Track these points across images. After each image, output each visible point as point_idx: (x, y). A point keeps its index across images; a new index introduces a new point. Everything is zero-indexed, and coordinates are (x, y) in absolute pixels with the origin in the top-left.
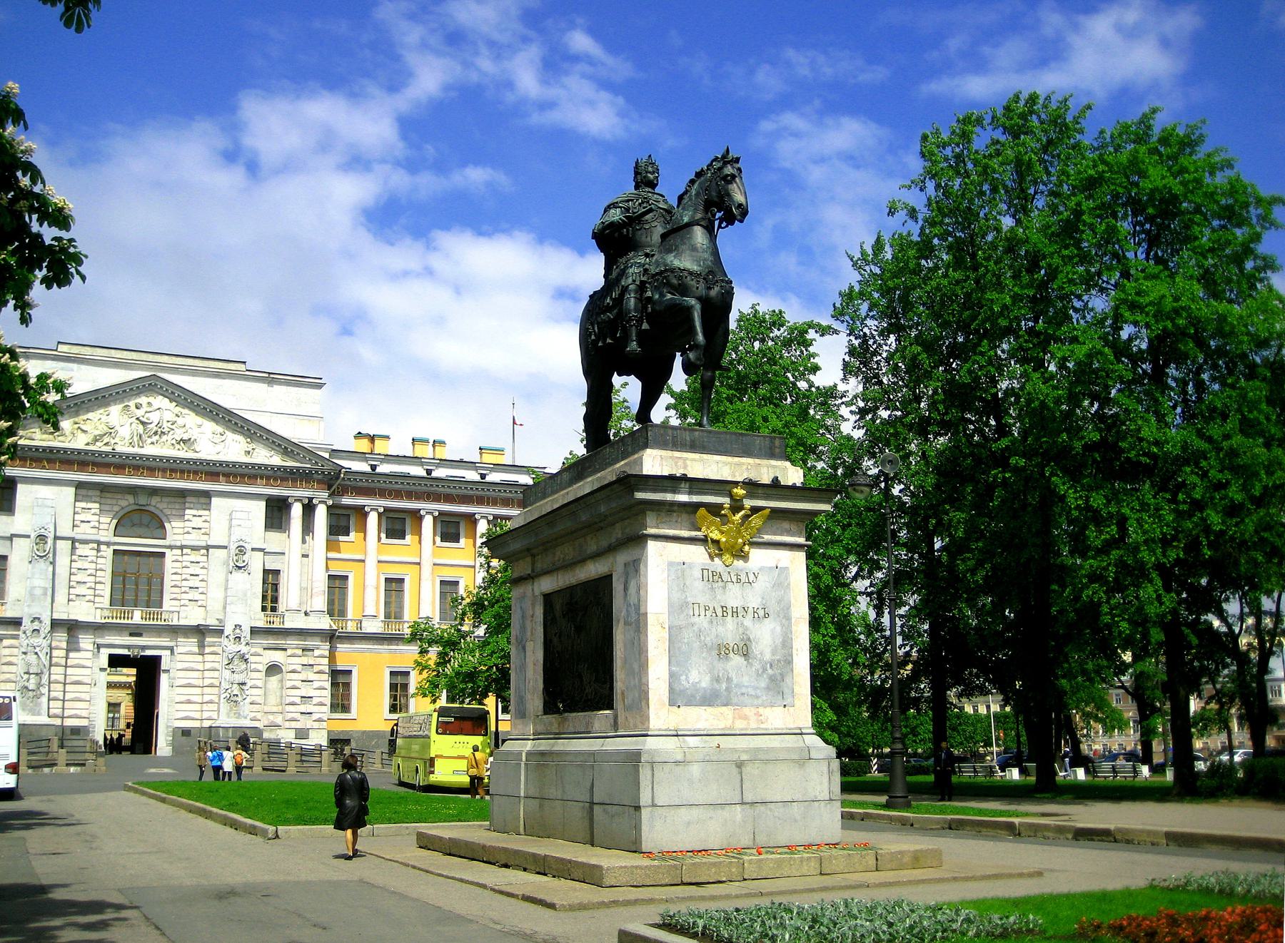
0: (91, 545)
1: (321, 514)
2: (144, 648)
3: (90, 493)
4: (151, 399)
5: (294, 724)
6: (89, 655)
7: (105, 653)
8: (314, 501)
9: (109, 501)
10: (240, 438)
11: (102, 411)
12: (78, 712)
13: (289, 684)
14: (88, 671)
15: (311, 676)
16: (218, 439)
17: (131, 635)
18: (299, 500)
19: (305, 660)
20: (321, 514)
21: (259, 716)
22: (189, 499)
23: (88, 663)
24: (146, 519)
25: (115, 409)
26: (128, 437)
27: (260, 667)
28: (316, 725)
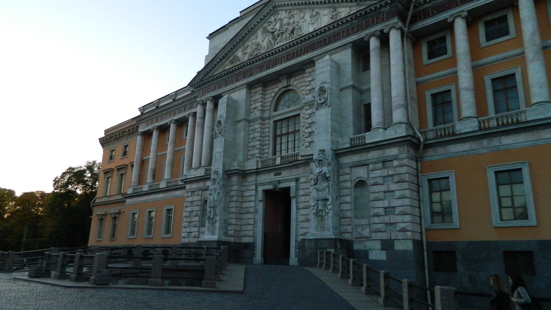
0: (257, 122)
1: (395, 38)
2: (279, 182)
3: (258, 89)
4: (276, 17)
5: (380, 236)
6: (253, 193)
7: (260, 189)
8: (385, 31)
9: (270, 92)
10: (326, 11)
11: (253, 37)
12: (246, 232)
13: (372, 196)
14: (252, 204)
15: (393, 187)
16: (313, 20)
17: (275, 175)
18: (373, 35)
19: (385, 172)
20: (395, 38)
21: (349, 229)
22: (307, 71)
23: (253, 198)
24: (291, 94)
25: (259, 32)
26: (266, 45)
27: (349, 184)
28: (400, 236)
